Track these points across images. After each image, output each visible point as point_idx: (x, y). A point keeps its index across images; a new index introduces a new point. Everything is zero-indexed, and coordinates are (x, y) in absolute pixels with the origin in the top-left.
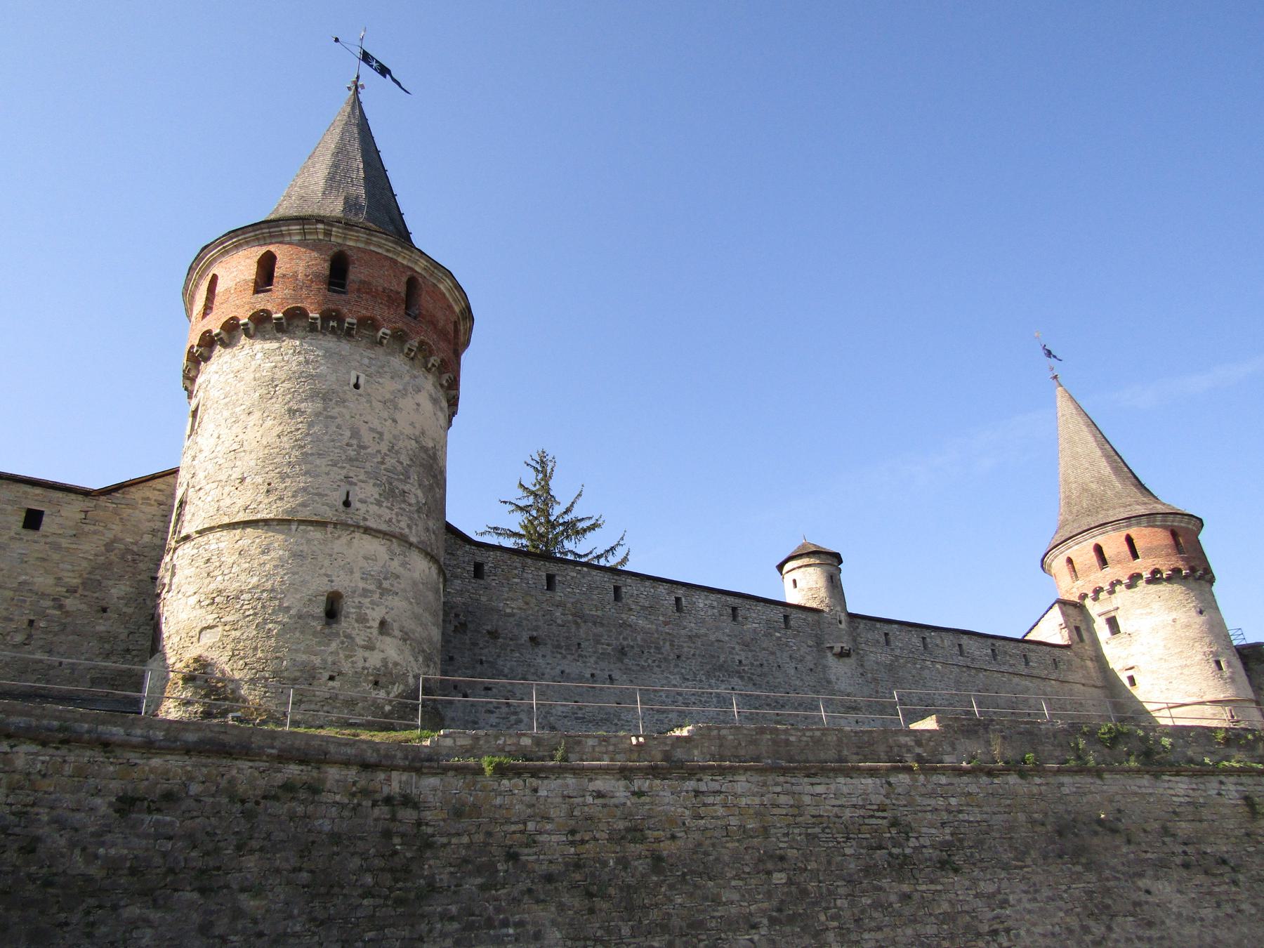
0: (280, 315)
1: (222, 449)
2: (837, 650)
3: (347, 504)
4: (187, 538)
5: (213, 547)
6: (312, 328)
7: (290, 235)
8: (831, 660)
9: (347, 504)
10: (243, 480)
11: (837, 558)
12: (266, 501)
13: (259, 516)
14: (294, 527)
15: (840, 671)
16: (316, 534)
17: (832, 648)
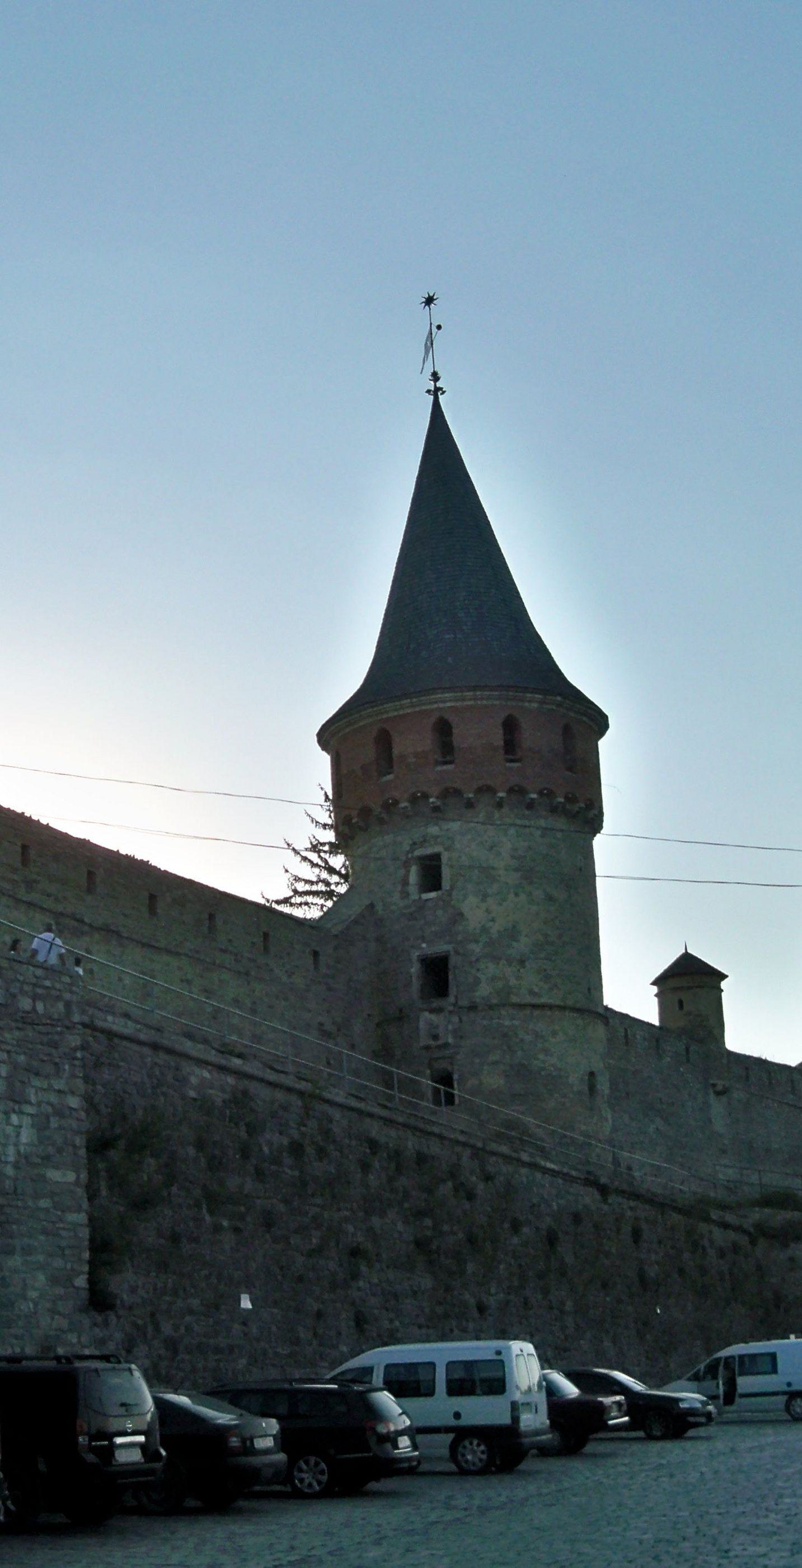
0: (534, 796)
1: (495, 928)
2: (719, 1088)
3: (589, 989)
4: (473, 1008)
5: (507, 1023)
6: (554, 810)
7: (530, 701)
8: (712, 1097)
9: (589, 989)
10: (522, 962)
11: (724, 977)
12: (546, 987)
13: (543, 1000)
14: (567, 1013)
15: (717, 1108)
16: (580, 1022)
17: (714, 1085)
